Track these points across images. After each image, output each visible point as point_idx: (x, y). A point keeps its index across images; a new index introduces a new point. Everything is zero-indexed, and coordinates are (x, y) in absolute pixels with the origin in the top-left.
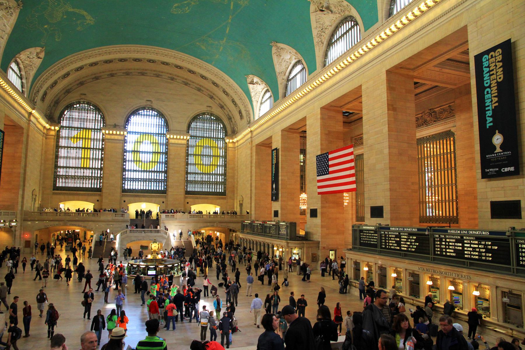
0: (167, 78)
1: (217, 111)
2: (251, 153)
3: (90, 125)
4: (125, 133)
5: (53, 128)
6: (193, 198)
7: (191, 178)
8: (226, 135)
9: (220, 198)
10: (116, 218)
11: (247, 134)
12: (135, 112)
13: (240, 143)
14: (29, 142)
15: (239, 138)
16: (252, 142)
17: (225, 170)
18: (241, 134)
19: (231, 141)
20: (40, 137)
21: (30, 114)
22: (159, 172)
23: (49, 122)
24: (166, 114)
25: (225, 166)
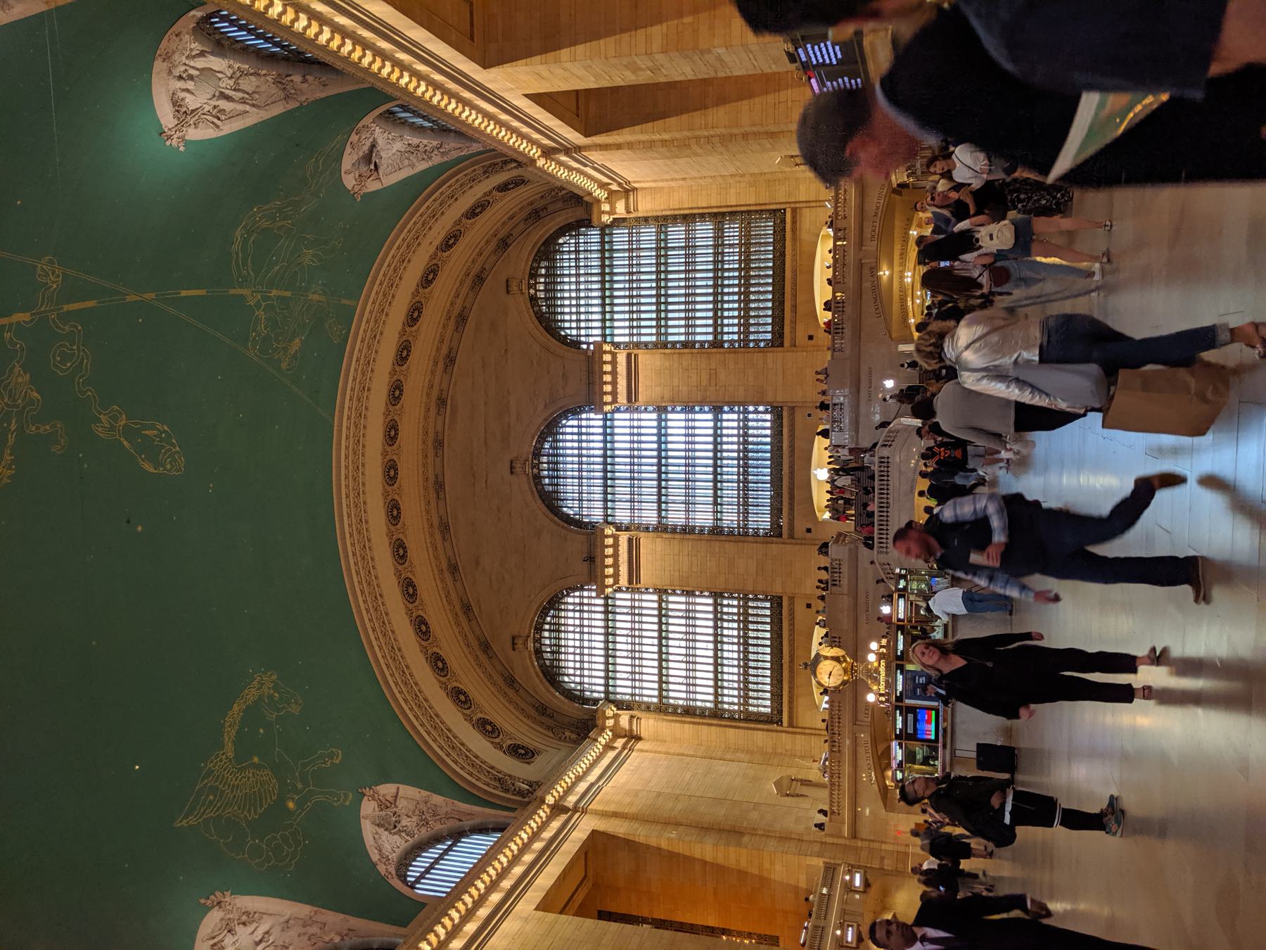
0: (440, 419)
1: (521, 256)
2: (619, 147)
4: (609, 531)
5: (610, 723)
6: (794, 322)
7: (731, 332)
8: (588, 224)
9: (794, 230)
10: (845, 582)
11: (560, 164)
13: (606, 180)
14: (633, 810)
16: (579, 149)
18: (568, 182)
19: (606, 207)
20: (634, 759)
21: (558, 809)
24: (545, 415)
25: (688, 219)
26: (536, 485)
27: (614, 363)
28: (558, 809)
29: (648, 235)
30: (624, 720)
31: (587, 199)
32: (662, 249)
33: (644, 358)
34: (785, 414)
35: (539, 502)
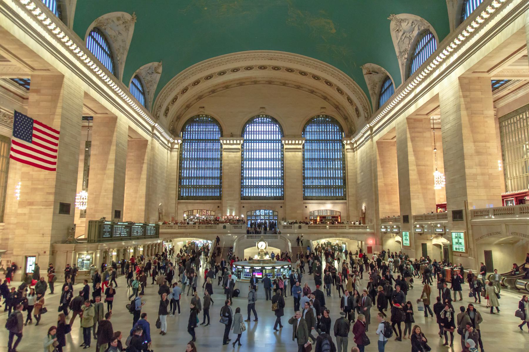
3: (210, 137)
5: (176, 142)
7: (308, 183)
12: (251, 121)
13: (358, 143)
15: (356, 138)
16: (372, 138)
17: (344, 173)
19: (349, 142)
21: (153, 128)
22: (275, 178)
23: (173, 136)
25: (344, 168)
26: (256, 116)
27: (298, 144)
28: (153, 128)
29: (338, 155)
30: (176, 146)
31: (352, 137)
32: (334, 160)
33: (300, 154)
34: (282, 201)
35: (250, 117)
